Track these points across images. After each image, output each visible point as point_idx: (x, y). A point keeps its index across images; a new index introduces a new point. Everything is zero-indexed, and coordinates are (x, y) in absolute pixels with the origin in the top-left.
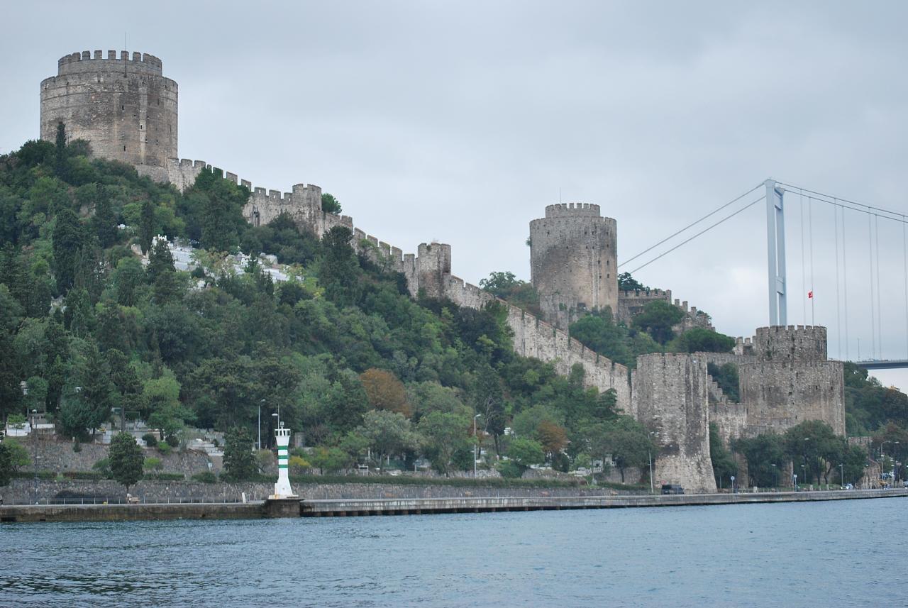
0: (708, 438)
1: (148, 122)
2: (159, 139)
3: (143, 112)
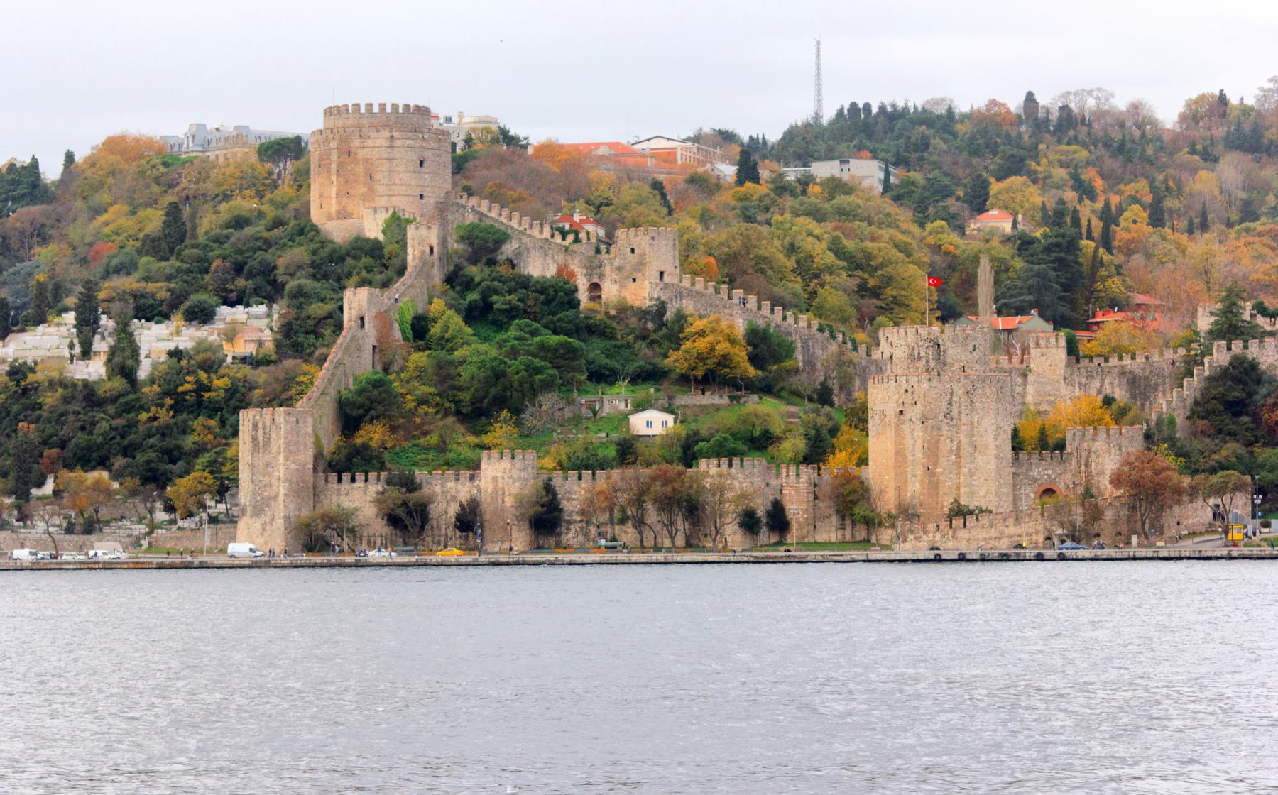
0: (281, 497)
1: (338, 176)
2: (351, 191)
3: (334, 166)
